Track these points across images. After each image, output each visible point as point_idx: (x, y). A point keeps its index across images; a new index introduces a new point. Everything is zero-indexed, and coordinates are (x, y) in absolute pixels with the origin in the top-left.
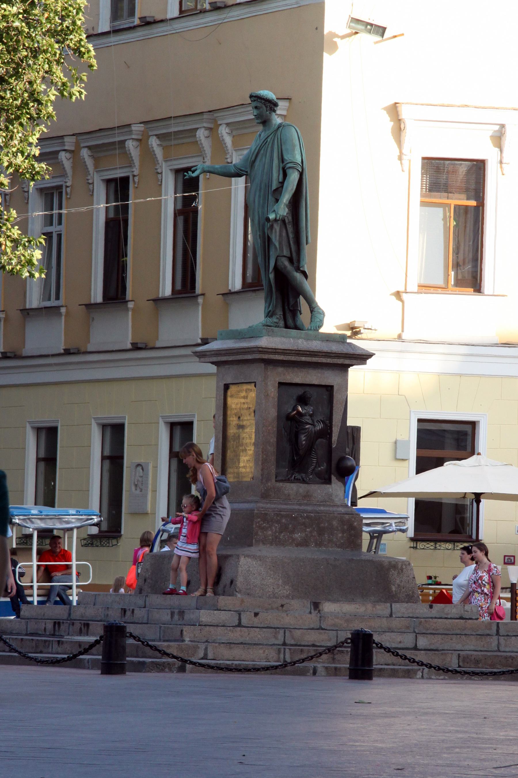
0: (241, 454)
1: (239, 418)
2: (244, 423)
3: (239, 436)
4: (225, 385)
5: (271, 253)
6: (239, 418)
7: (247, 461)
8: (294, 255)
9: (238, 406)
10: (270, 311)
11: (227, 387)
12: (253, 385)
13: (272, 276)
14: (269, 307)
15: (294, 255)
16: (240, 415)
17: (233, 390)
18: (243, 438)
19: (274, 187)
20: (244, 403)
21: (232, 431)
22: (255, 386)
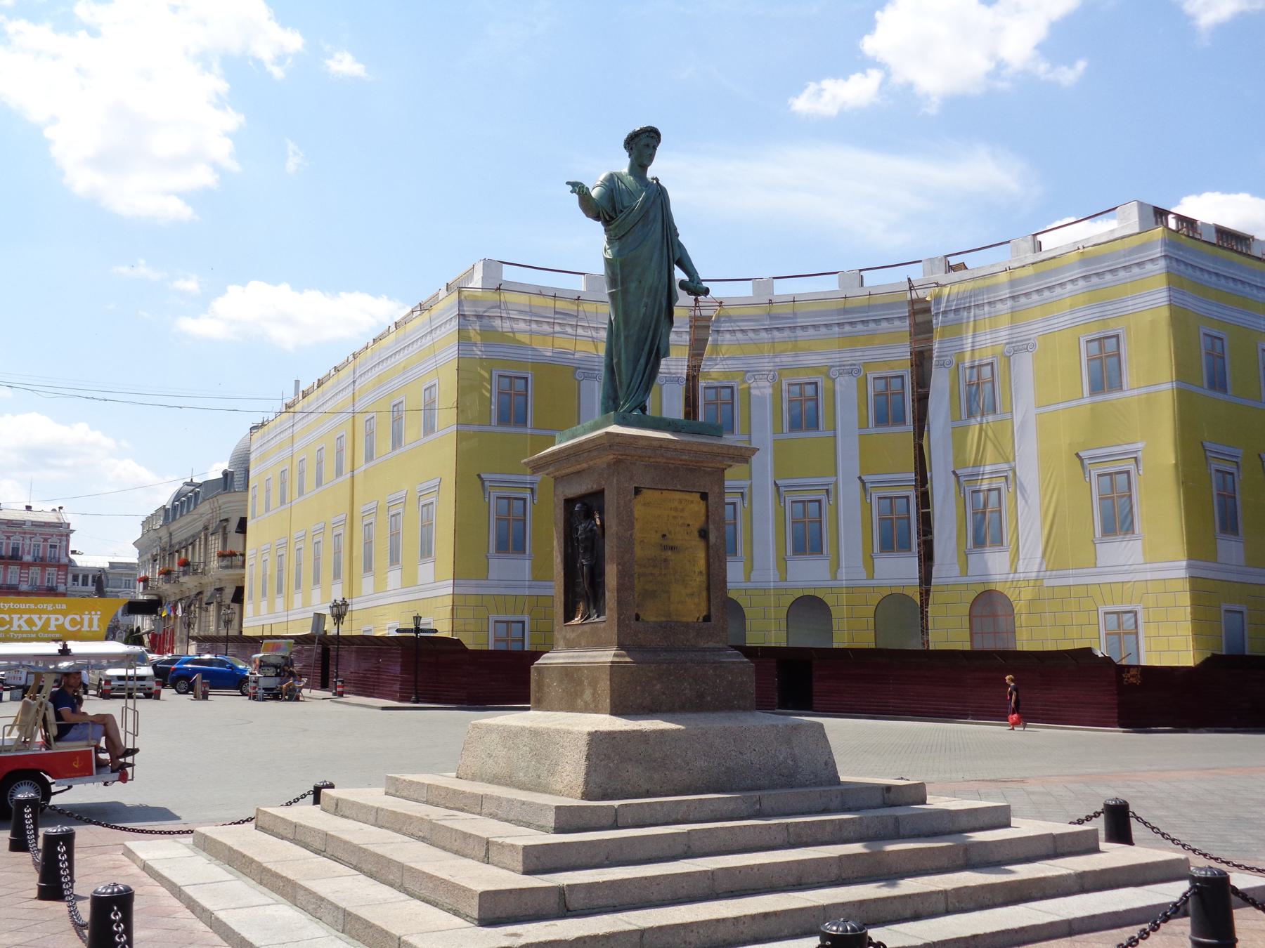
3: (666, 560)
6: (664, 536)
11: (637, 491)
12: (698, 495)
20: (675, 517)
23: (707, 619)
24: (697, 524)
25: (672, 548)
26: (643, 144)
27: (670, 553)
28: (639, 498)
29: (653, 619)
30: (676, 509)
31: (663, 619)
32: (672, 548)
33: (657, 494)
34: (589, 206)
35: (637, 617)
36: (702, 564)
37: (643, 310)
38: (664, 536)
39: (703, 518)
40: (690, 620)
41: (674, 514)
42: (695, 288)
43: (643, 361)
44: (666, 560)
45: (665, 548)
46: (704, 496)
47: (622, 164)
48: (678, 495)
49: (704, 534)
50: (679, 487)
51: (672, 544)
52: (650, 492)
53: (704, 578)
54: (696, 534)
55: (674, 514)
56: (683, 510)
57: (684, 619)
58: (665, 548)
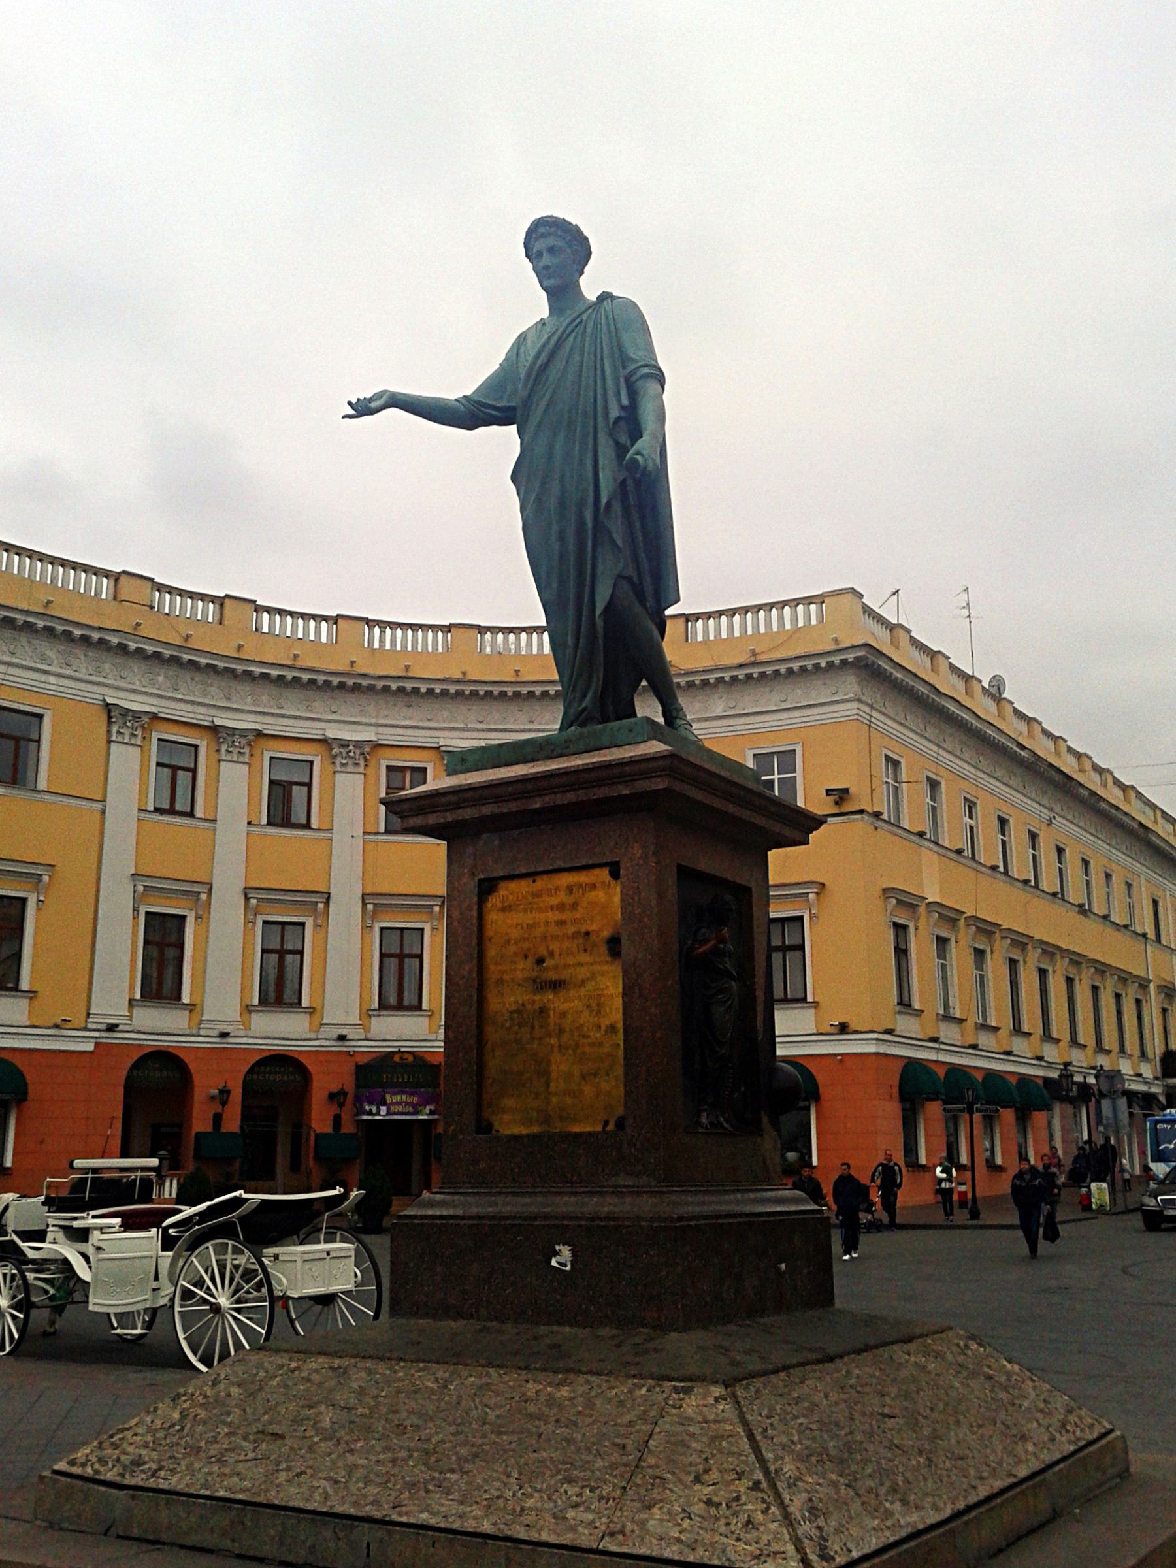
0: (556, 1057)
1: (540, 961)
2: (564, 975)
3: (543, 1011)
4: (480, 881)
5: (600, 568)
7: (583, 1077)
8: (648, 582)
9: (539, 932)
10: (584, 709)
11: (487, 887)
12: (604, 874)
13: (600, 623)
14: (580, 703)
15: (648, 582)
16: (543, 951)
17: (509, 891)
18: (563, 1015)
19: (615, 413)
20: (561, 923)
21: (503, 1001)
22: (615, 875)
24: (606, 934)
25: (557, 985)
28: (494, 901)
29: (517, 1130)
30: (561, 907)
31: (536, 1129)
33: (522, 887)
35: (484, 1127)
37: (556, 546)
41: (557, 916)
44: (543, 1011)
49: (614, 945)
50: (560, 864)
51: (552, 976)
52: (513, 885)
53: (620, 1037)
54: (603, 949)
55: (557, 916)
56: (574, 906)
57: (576, 1129)
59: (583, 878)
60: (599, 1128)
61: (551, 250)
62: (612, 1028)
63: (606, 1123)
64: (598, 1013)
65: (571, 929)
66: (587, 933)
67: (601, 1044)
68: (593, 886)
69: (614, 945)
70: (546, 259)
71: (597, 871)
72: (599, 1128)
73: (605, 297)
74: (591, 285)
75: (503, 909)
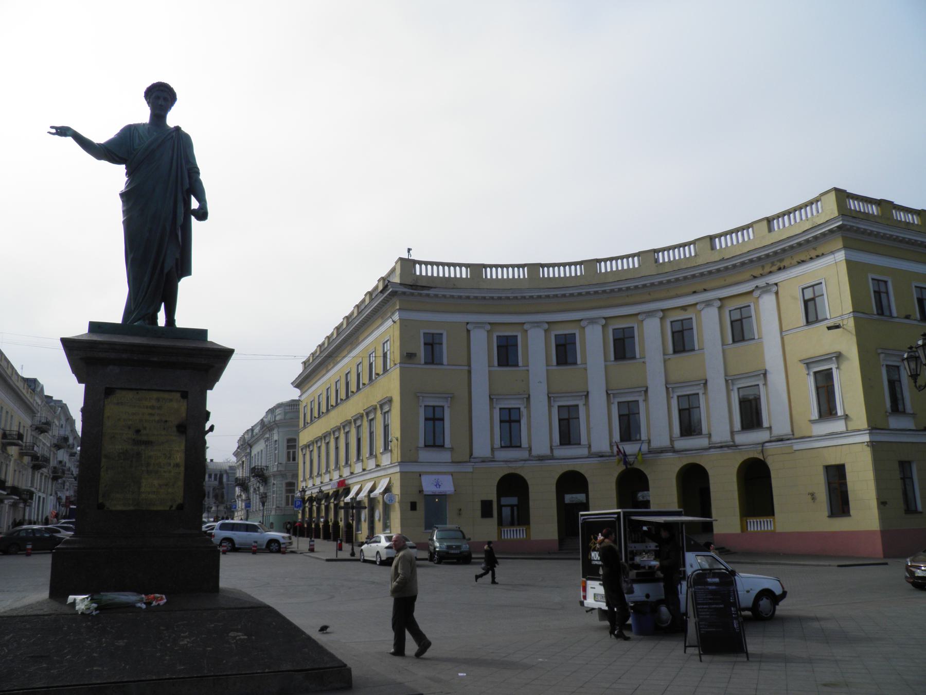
1: (138, 431)
4: (107, 389)
11: (109, 392)
12: (178, 395)
18: (150, 457)
20: (151, 414)
23: (180, 507)
25: (148, 443)
26: (161, 96)
27: (143, 447)
29: (119, 508)
30: (153, 407)
31: (132, 508)
32: (148, 443)
33: (130, 395)
34: (106, 152)
35: (101, 506)
36: (179, 457)
38: (138, 431)
39: (184, 415)
40: (160, 508)
42: (202, 215)
43: (146, 279)
45: (137, 442)
46: (184, 395)
47: (142, 114)
48: (155, 395)
49: (182, 429)
54: (175, 429)
56: (160, 408)
57: (155, 508)
58: (137, 442)
59: (166, 395)
60: (168, 508)
61: (165, 99)
62: (177, 465)
63: (171, 507)
64: (170, 458)
65: (157, 418)
66: (166, 421)
67: (170, 472)
68: (171, 400)
69: (182, 429)
70: (161, 102)
71: (173, 394)
72: (168, 508)
73: (178, 129)
74: (173, 119)
75: (118, 404)
